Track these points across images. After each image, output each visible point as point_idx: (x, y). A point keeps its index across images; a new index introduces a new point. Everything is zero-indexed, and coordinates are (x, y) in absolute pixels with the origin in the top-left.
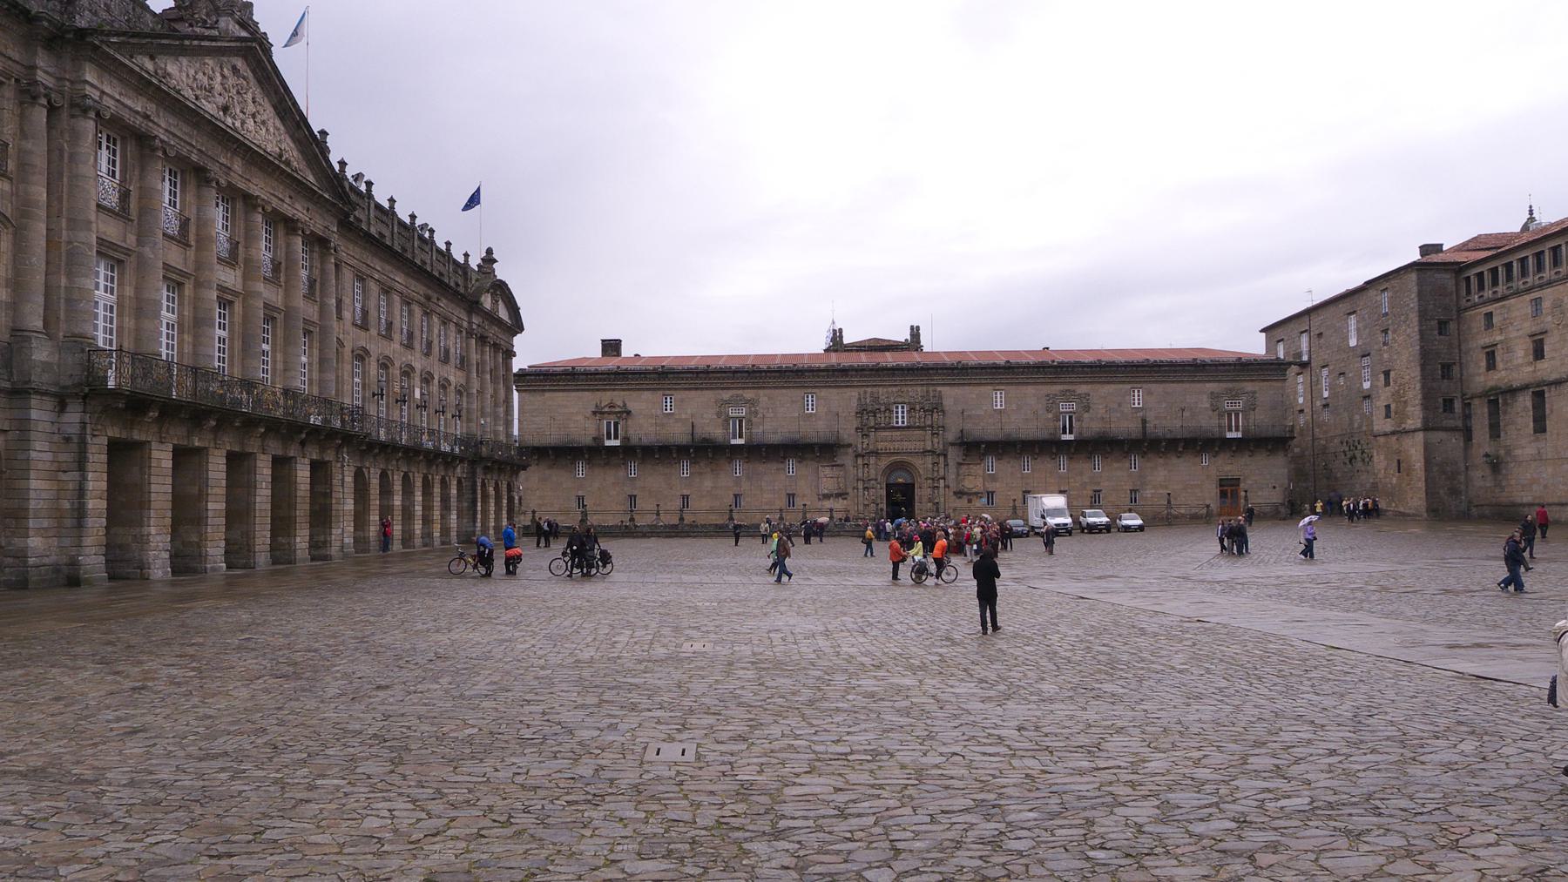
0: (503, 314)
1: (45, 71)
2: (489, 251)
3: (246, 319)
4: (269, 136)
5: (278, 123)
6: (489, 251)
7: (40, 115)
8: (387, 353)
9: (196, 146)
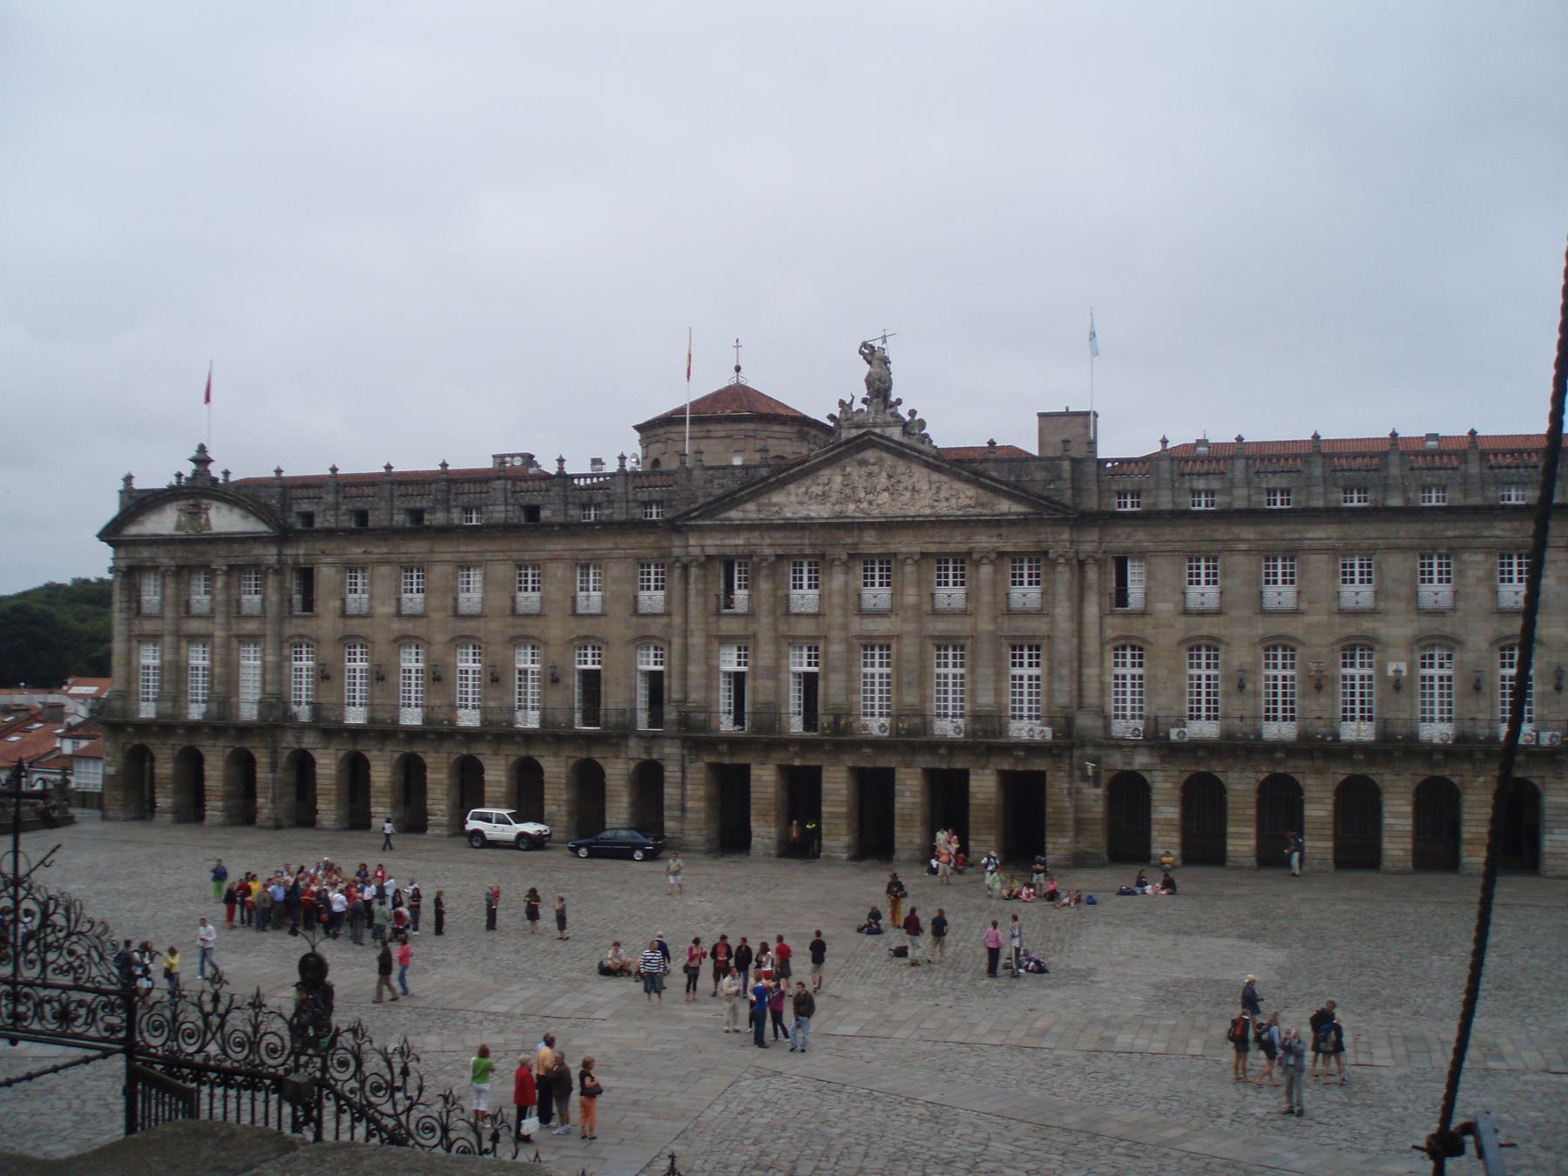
3: (899, 659)
4: (928, 495)
5: (936, 477)
7: (677, 573)
8: (1282, 631)
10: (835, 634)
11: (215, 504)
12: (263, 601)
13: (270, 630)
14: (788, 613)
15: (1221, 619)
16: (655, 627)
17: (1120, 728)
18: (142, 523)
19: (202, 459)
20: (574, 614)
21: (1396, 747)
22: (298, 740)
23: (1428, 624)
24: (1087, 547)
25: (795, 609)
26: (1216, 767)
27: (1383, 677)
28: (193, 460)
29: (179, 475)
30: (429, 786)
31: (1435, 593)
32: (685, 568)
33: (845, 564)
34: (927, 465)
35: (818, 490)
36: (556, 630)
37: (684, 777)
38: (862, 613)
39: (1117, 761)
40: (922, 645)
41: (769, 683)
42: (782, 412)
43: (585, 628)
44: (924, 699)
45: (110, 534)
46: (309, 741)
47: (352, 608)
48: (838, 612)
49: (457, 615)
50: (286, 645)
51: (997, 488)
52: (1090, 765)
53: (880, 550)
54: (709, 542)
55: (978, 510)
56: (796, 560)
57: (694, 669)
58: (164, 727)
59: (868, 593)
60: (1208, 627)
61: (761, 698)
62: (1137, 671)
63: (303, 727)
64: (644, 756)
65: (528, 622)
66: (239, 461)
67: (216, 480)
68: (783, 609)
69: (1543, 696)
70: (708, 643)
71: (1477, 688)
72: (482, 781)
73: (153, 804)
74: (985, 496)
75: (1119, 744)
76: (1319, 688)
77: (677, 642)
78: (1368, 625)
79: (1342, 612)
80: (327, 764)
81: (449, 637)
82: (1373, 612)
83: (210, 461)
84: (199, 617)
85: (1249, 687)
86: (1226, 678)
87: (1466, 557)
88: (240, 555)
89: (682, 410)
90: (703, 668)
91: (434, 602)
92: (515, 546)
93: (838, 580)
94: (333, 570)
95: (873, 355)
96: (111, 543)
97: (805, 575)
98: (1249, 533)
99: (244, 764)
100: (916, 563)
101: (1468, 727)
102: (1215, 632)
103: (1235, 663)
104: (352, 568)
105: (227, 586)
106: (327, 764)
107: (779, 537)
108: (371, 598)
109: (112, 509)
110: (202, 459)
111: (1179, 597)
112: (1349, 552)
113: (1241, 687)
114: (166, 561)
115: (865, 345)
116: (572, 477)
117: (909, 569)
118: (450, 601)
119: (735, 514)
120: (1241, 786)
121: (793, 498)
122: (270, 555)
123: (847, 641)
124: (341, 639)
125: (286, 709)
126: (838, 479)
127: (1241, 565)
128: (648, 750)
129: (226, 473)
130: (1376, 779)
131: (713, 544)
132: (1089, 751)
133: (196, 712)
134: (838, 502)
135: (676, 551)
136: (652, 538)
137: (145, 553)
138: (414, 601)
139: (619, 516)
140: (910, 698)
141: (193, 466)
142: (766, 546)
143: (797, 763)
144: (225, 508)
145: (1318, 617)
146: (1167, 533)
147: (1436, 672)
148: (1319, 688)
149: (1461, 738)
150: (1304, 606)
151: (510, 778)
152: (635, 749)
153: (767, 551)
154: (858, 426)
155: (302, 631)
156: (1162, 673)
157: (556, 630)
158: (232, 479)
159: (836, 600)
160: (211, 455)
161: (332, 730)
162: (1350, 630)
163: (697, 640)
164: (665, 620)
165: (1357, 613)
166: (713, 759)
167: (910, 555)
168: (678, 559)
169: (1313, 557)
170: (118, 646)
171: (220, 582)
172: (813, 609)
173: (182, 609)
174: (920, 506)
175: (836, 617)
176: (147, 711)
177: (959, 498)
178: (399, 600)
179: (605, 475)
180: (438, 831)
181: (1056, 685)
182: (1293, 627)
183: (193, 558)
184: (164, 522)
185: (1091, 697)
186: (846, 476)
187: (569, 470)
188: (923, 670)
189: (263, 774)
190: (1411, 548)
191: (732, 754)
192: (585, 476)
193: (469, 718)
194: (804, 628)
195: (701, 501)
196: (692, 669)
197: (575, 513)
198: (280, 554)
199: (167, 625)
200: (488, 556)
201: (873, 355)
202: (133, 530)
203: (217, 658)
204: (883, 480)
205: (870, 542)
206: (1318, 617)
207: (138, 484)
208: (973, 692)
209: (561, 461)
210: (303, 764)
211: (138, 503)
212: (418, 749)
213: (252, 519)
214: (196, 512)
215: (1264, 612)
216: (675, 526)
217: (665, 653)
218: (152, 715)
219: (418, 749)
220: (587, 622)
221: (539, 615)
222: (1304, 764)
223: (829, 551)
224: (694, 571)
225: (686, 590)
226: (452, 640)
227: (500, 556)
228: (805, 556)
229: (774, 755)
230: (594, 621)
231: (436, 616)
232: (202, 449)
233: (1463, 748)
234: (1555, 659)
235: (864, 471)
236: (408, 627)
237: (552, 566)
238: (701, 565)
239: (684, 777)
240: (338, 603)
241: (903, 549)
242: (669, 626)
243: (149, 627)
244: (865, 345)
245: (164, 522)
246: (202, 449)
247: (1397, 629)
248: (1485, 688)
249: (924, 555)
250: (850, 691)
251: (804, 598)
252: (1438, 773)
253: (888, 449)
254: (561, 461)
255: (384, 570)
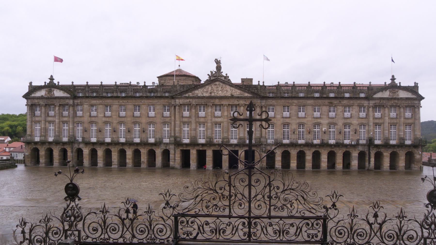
0: (403, 94)
1: (173, 102)
2: (393, 76)
3: (223, 127)
5: (232, 88)
6: (393, 76)
7: (173, 108)
9: (203, 101)
10: (209, 121)
11: (55, 90)
12: (69, 113)
13: (71, 120)
14: (198, 117)
15: (290, 119)
16: (167, 120)
17: (269, 141)
18: (35, 94)
19: (52, 79)
20: (148, 117)
21: (324, 145)
22: (78, 146)
23: (331, 120)
24: (263, 104)
25: (200, 116)
26: (289, 149)
27: (322, 131)
28: (49, 79)
29: (45, 83)
30: (112, 156)
31: (332, 114)
32: (175, 107)
33: (211, 106)
34: (230, 85)
35: (206, 90)
36: (144, 120)
37: (175, 152)
38: (215, 117)
39: (269, 148)
40: (228, 124)
41: (194, 132)
42: (184, 73)
43: (151, 120)
44: (228, 135)
45: (26, 96)
46: (81, 146)
47: (92, 115)
48: (210, 117)
49: (119, 116)
50: (75, 124)
51: (245, 92)
52: (264, 149)
53: (219, 103)
54: (181, 101)
55: (241, 95)
56: (200, 105)
57: (177, 129)
58: (43, 143)
59: (216, 113)
60: (288, 120)
61: (192, 135)
62: (273, 130)
63: (80, 143)
64: (165, 148)
65: (137, 118)
66: (63, 79)
67: (55, 84)
68: (197, 116)
69: (352, 135)
70: (180, 123)
71: (340, 133)
72: (126, 155)
73: (40, 162)
74: (242, 92)
75: (269, 145)
76: (309, 133)
77: (173, 123)
78: (319, 120)
79: (314, 118)
80: (86, 151)
81: (117, 122)
82: (320, 118)
83: (54, 79)
84: (51, 117)
85: (295, 133)
86: (291, 131)
87: (338, 107)
88: (63, 102)
89: (173, 71)
90: (179, 129)
91: (113, 114)
92: (134, 101)
93: (210, 110)
94: (87, 106)
95: (218, 62)
96: (26, 98)
97: (202, 109)
98: (295, 101)
99: (64, 152)
100: (227, 106)
101: (339, 141)
102: (289, 121)
103: (293, 128)
104: (92, 106)
105: (59, 109)
106: (86, 151)
107: (197, 100)
108: (97, 113)
109: (27, 90)
110: (52, 79)
111: (281, 114)
112: (316, 106)
113: (294, 133)
114: (42, 103)
115: (216, 59)
116: (148, 86)
117: (225, 108)
118: (118, 113)
119: (187, 95)
120: (294, 153)
121: (200, 92)
122: (71, 102)
123: (212, 123)
124: (89, 122)
125: (75, 139)
126: (210, 88)
127: (294, 108)
128: (166, 147)
129: (58, 82)
130: (320, 151)
131: (181, 101)
132: (263, 146)
133: (51, 139)
134: (211, 93)
135: (172, 103)
136: (167, 100)
137: (36, 101)
138: (108, 113)
139: (159, 95)
140: (226, 135)
141: (49, 80)
142: (194, 102)
143: (201, 149)
144: (58, 91)
145: (309, 119)
146: (279, 101)
147: (332, 130)
148: (309, 133)
149: (337, 143)
150: (306, 116)
151: (133, 154)
152: (163, 147)
153: (194, 103)
154: (215, 77)
155: (79, 120)
156: (278, 130)
157: (144, 120)
158: (60, 84)
159: (209, 114)
160: (54, 78)
161: (87, 143)
162: (315, 121)
163: (178, 123)
164: (170, 118)
165: (317, 118)
166: (182, 149)
167: (226, 105)
168: (173, 105)
169: (308, 107)
170: (28, 124)
171: (57, 108)
172: (204, 116)
173: (46, 115)
174: (229, 94)
175: (209, 118)
176: (37, 139)
177: (237, 93)
178: (105, 113)
179: (155, 86)
180: (115, 166)
181: (257, 132)
182: (304, 121)
183: (49, 102)
184: (42, 93)
185: (263, 135)
186: (212, 87)
187: (146, 85)
188: (228, 129)
189: (69, 154)
190: (328, 105)
191: (186, 147)
192: (151, 86)
193: (122, 140)
194: (202, 120)
195: (179, 92)
196: (177, 129)
197: (149, 94)
198: (73, 102)
199: (42, 119)
200: (127, 103)
201: (218, 62)
202: (33, 95)
203: (56, 126)
204: (220, 89)
205: (217, 102)
206: (309, 119)
207: (33, 84)
208: (239, 134)
209: (145, 82)
210: (80, 152)
211: (33, 89)
212: (110, 147)
213: (66, 93)
214: (50, 91)
215: (299, 118)
216: (172, 98)
217: (170, 125)
218: (39, 140)
219: (110, 147)
220: (151, 119)
221: (140, 117)
222: (306, 148)
223: (208, 103)
224: (177, 107)
225: (175, 112)
226: (118, 123)
227: (130, 103)
228: (202, 104)
229: (196, 147)
230: (153, 118)
231: (114, 117)
232: (52, 76)
233: (338, 145)
234: (355, 127)
235: (216, 86)
236: (107, 119)
237: (142, 106)
238: (179, 106)
239: (175, 152)
240: (89, 114)
241: (224, 103)
242: (171, 119)
243: (37, 119)
244: (216, 59)
245: (42, 93)
246: (52, 76)
247: (325, 121)
248: (342, 133)
249: (229, 105)
250: (212, 134)
251: (202, 114)
252: (332, 150)
253: (221, 82)
254: (145, 82)
255: (101, 106)
